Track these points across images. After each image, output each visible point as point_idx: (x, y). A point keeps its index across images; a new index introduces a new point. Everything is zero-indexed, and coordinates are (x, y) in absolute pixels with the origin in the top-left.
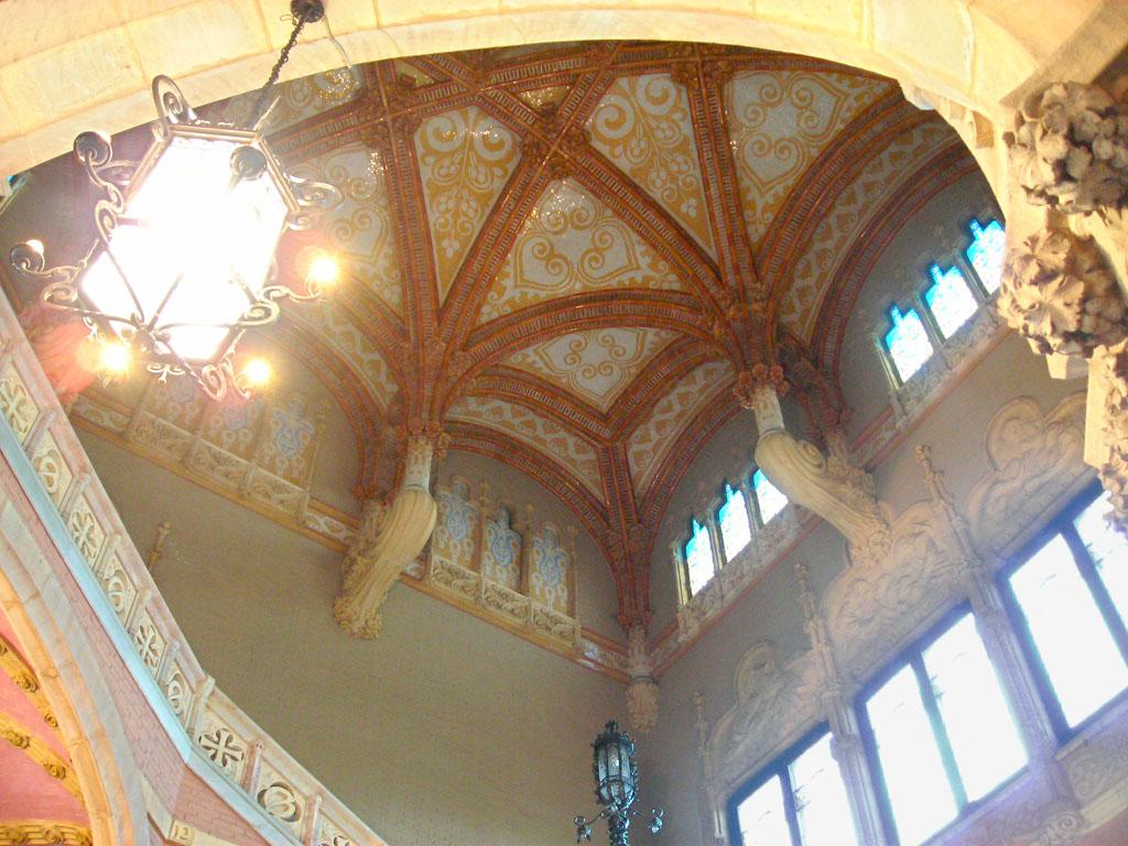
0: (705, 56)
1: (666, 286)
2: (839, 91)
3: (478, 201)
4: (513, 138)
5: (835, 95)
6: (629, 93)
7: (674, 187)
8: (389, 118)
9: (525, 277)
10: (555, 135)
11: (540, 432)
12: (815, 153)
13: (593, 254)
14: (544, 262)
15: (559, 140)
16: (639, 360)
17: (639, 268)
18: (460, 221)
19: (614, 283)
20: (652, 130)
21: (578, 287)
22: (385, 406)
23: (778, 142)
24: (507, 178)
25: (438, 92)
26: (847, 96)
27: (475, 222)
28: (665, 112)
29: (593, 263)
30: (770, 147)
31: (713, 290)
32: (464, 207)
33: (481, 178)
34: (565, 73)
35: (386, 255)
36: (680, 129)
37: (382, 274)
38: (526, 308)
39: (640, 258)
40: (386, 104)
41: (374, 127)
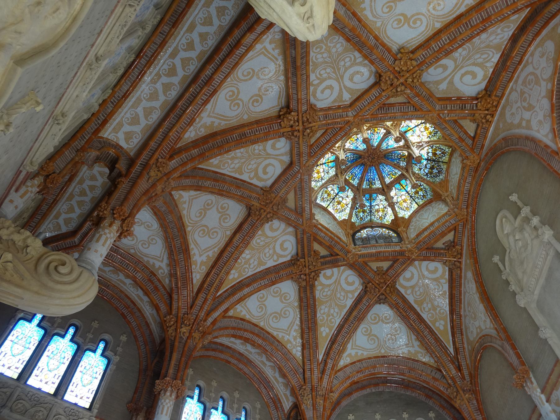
0: (309, 275)
1: (194, 275)
2: (291, 330)
3: (238, 168)
4: (269, 179)
5: (288, 328)
6: (286, 232)
7: (243, 263)
8: (301, 128)
9: (194, 200)
10: (275, 210)
11: (77, 198)
12: (262, 324)
13: (206, 230)
14: (202, 207)
15: (272, 211)
16: (139, 254)
17: (201, 256)
18: (229, 161)
19: (192, 246)
20: (268, 246)
21: (189, 229)
22: (105, 136)
23: (264, 305)
24: (248, 180)
25: (304, 149)
26: (289, 335)
27: (228, 169)
28: (277, 252)
29: (202, 232)
30: (262, 301)
31: (202, 314)
32: (236, 161)
33: (250, 167)
34: (303, 209)
35: (213, 123)
36: (269, 260)
37: (202, 122)
38: (177, 207)
39: (206, 254)
40: (311, 125)
41: (298, 122)
